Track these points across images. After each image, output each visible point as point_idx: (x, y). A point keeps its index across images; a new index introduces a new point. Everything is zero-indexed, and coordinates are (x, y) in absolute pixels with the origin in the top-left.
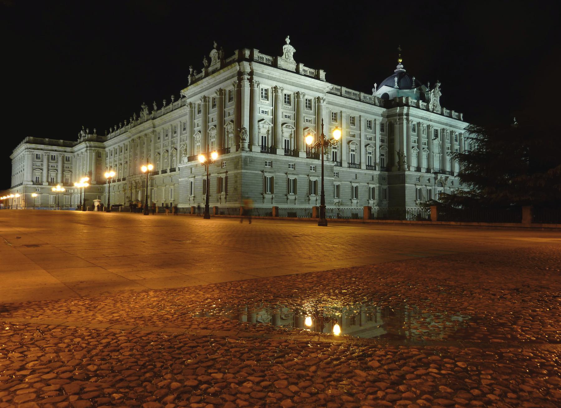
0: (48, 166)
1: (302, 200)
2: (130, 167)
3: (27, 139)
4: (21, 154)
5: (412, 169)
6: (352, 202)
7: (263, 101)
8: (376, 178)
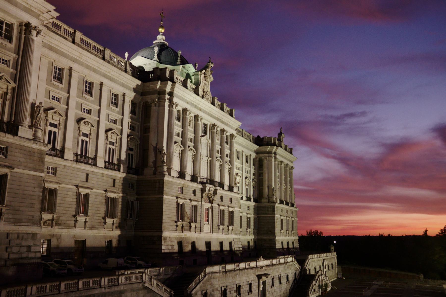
5: (174, 173)
6: (76, 221)
8: (119, 184)
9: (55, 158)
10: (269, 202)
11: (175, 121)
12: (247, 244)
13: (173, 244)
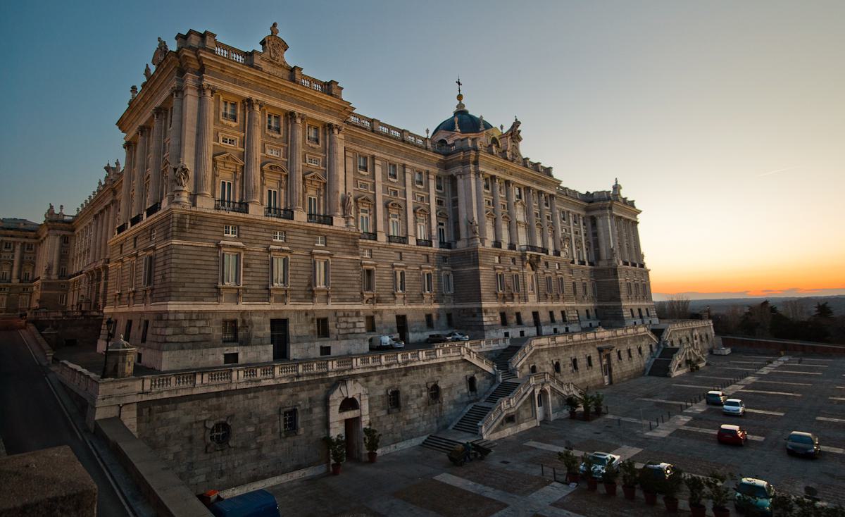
1: (300, 296)
7: (225, 122)
9: (369, 241)
11: (483, 189)
12: (585, 313)
13: (495, 315)
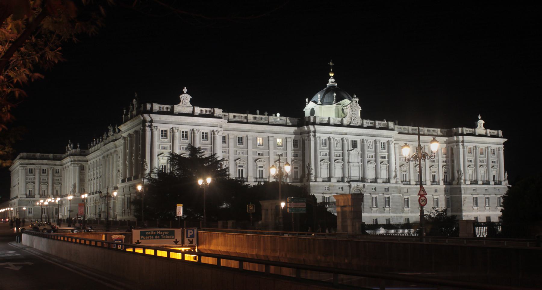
0: (40, 179)
2: (100, 182)
3: (21, 155)
4: (17, 168)
10: (458, 184)
